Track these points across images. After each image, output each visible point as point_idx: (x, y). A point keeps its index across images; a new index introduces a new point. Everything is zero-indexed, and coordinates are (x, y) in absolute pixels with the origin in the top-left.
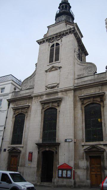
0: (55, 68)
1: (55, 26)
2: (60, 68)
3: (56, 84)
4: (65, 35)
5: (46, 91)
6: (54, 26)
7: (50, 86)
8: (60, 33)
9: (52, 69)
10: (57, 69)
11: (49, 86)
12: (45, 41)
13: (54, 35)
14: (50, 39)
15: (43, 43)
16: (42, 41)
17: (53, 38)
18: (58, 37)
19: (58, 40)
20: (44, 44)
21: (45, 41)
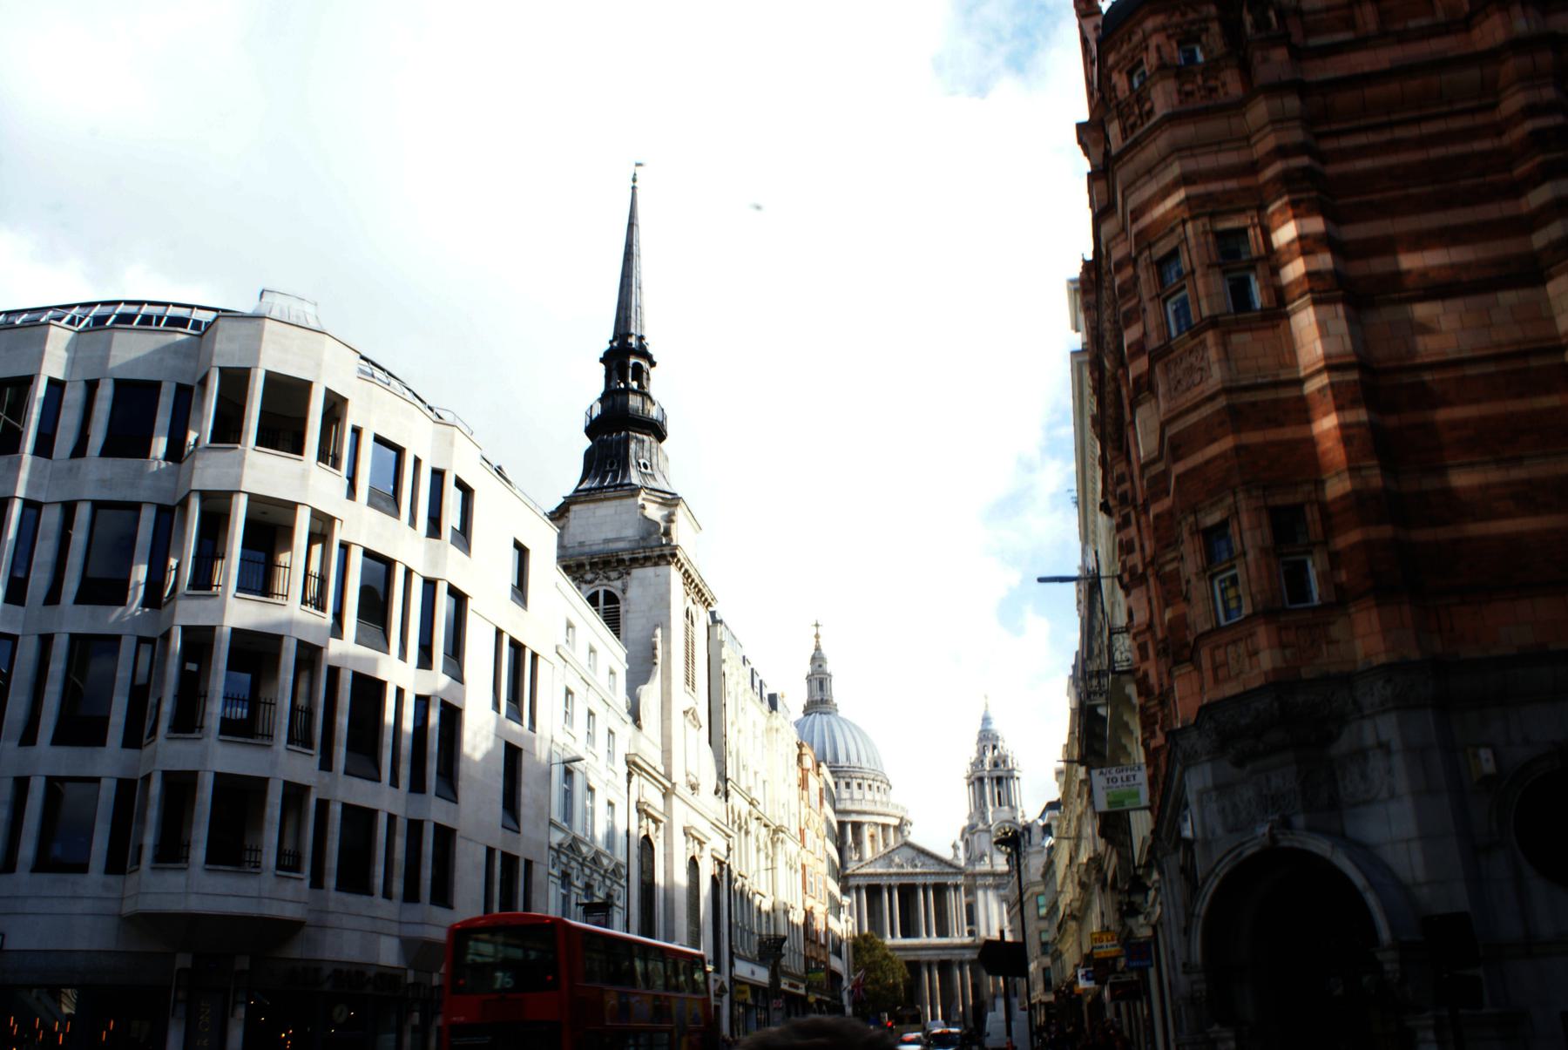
0: (694, 719)
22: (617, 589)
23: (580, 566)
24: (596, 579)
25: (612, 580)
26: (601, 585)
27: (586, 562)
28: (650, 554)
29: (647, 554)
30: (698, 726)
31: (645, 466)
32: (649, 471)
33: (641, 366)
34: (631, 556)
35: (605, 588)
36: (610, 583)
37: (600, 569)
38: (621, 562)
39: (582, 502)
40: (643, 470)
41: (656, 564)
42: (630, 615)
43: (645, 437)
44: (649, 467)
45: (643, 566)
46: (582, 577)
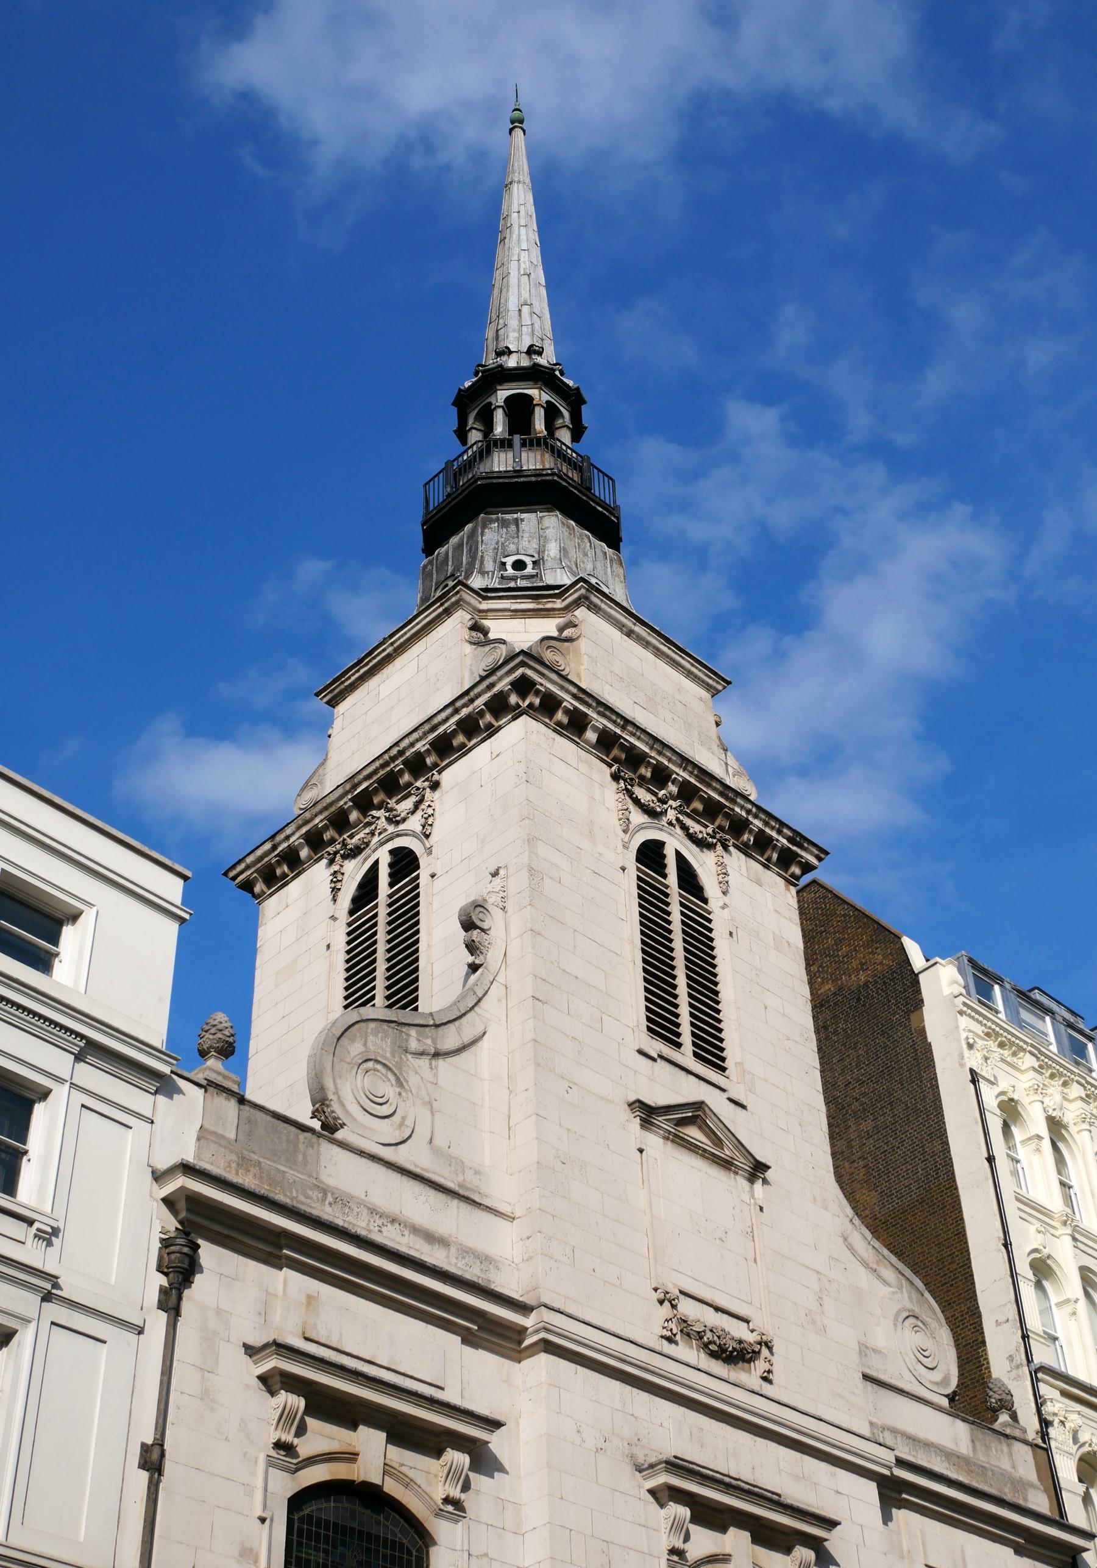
0: (718, 1142)
1: (639, 639)
2: (758, 1170)
3: (738, 1331)
4: (745, 849)
5: (668, 1348)
6: (630, 633)
7: (713, 1319)
8: (725, 789)
9: (682, 1122)
10: (726, 1164)
11: (687, 1308)
12: (591, 736)
13: (685, 762)
14: (634, 759)
15: (560, 729)
16: (569, 702)
17: (661, 777)
18: (698, 805)
19: (701, 844)
20: (564, 746)
21: (591, 736)
22: (414, 834)
23: (340, 822)
24: (372, 834)
25: (404, 820)
26: (382, 844)
27: (346, 802)
28: (470, 708)
29: (465, 712)
30: (741, 1162)
31: (519, 565)
32: (529, 570)
33: (530, 398)
34: (431, 736)
35: (391, 845)
36: (402, 827)
37: (379, 808)
38: (417, 766)
39: (353, 687)
40: (510, 571)
41: (492, 731)
42: (438, 883)
43: (524, 516)
44: (530, 566)
45: (464, 751)
46: (344, 844)
